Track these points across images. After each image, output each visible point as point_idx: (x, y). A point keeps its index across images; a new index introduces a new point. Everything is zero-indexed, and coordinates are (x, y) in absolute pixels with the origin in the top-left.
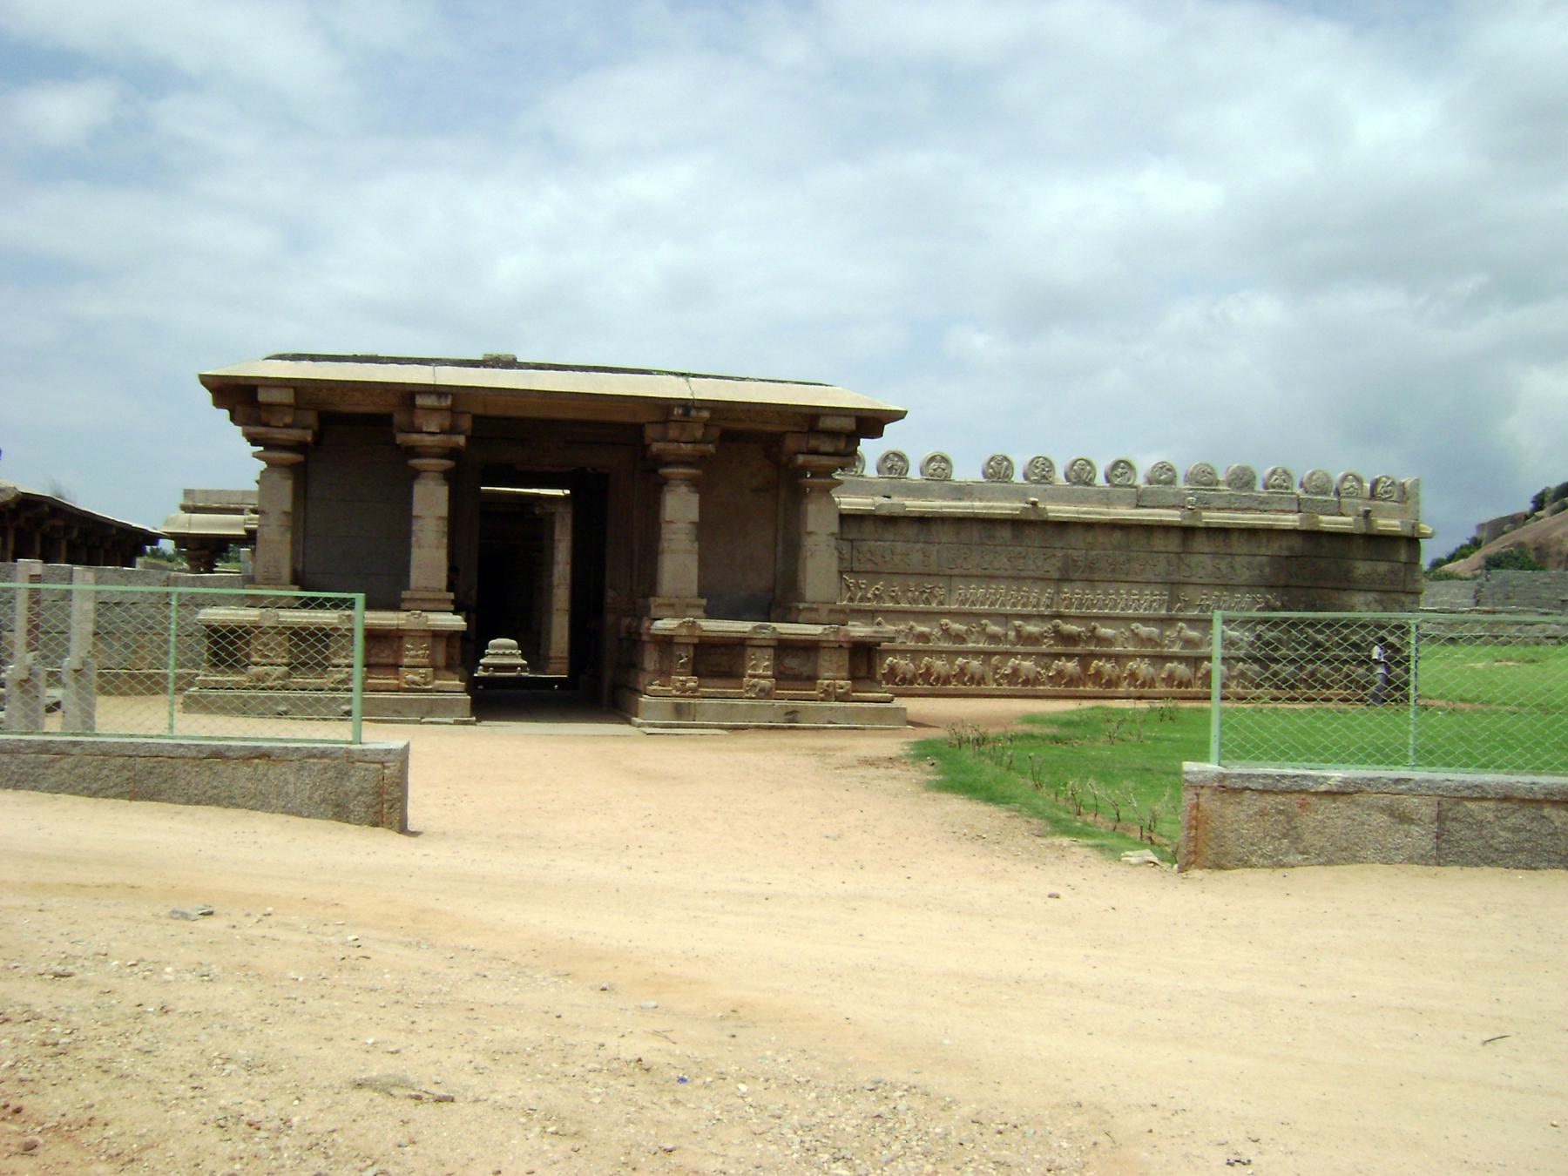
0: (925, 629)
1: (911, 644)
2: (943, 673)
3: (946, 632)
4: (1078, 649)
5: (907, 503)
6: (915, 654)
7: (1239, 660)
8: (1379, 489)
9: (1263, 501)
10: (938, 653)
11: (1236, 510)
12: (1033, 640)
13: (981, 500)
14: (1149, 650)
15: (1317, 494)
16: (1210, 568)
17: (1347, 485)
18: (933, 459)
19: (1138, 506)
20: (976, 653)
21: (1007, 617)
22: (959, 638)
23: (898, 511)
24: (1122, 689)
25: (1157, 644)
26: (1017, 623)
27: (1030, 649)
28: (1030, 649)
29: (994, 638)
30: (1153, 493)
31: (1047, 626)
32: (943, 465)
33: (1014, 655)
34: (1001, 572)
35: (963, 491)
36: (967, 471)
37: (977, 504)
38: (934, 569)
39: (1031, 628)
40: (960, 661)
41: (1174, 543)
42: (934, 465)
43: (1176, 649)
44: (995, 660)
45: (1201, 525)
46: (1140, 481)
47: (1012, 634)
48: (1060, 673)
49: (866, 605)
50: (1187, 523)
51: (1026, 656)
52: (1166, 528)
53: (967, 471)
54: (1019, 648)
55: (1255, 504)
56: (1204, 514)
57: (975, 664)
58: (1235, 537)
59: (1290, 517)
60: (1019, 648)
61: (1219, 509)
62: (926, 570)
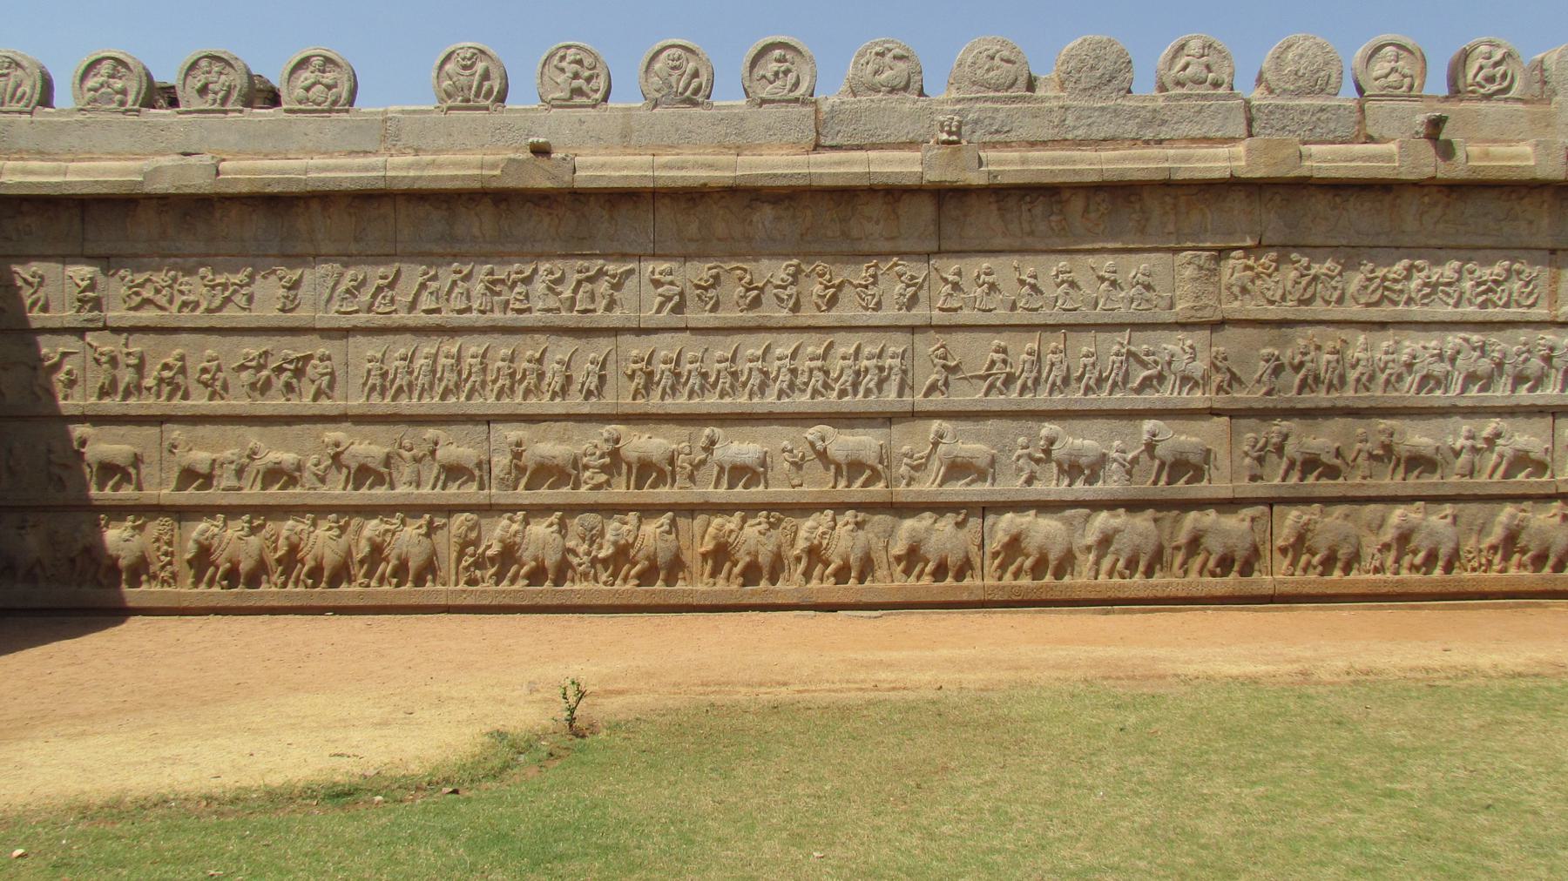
0: (288, 458)
1: (252, 493)
4: (665, 494)
7: (1096, 506)
9: (1156, 118)
11: (1080, 143)
14: (857, 491)
15: (1298, 93)
16: (1009, 290)
17: (1380, 67)
18: (303, 63)
19: (817, 147)
24: (790, 585)
26: (513, 433)
30: (856, 116)
34: (473, 318)
35: (387, 132)
38: (302, 315)
39: (549, 446)
40: (373, 527)
42: (306, 76)
43: (928, 486)
45: (976, 178)
46: (831, 96)
48: (622, 553)
49: (134, 405)
50: (933, 176)
54: (523, 495)
55: (1131, 129)
57: (408, 537)
58: (1077, 204)
59: (1223, 151)
62: (288, 320)
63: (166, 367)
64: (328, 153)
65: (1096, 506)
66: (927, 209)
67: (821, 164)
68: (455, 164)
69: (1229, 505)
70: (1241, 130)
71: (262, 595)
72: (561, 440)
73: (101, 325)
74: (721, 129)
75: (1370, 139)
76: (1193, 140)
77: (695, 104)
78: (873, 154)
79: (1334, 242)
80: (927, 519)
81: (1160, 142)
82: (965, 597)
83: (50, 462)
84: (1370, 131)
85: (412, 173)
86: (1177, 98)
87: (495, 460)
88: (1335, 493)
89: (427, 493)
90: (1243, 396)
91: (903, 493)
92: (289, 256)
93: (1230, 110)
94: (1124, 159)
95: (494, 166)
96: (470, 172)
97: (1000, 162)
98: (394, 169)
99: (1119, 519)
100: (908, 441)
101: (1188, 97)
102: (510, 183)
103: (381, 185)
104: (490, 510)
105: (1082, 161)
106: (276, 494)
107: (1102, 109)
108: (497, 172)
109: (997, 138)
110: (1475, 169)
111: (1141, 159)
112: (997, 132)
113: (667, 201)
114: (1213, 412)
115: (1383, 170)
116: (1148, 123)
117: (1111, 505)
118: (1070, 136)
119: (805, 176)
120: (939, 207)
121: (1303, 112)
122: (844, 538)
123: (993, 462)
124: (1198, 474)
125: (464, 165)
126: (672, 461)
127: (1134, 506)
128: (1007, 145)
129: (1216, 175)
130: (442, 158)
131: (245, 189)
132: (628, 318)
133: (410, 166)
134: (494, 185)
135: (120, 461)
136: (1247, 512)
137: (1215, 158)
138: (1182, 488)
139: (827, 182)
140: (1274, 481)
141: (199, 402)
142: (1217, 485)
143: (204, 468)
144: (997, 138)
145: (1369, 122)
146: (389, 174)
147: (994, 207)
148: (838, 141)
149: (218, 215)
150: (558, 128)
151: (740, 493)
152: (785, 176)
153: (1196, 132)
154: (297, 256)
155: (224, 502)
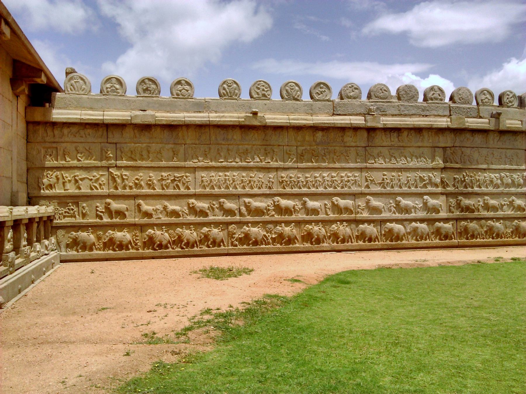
0: (177, 208)
2: (192, 240)
3: (193, 210)
4: (294, 217)
5: (157, 114)
6: (169, 226)
8: (505, 100)
10: (188, 225)
11: (406, 115)
12: (259, 212)
13: (216, 112)
19: (333, 114)
20: (217, 224)
21: (239, 196)
22: (203, 213)
23: (151, 121)
25: (351, 212)
26: (247, 200)
27: (257, 219)
28: (257, 219)
29: (229, 212)
31: (270, 202)
32: (187, 87)
33: (247, 223)
36: (206, 91)
37: (214, 115)
39: (256, 203)
40: (205, 229)
41: (362, 139)
43: (365, 215)
44: (231, 227)
45: (380, 126)
47: (243, 209)
49: (127, 191)
51: (255, 224)
52: (356, 129)
53: (206, 91)
56: (382, 118)
57: (215, 231)
58: (405, 133)
59: (445, 119)
60: (249, 218)
61: (393, 115)
63: (137, 179)
64: (188, 111)
65: (411, 220)
66: (365, 134)
67: (337, 120)
68: (230, 117)
69: (446, 220)
70: (448, 114)
71: (169, 252)
72: (261, 202)
73: (114, 165)
74: (306, 108)
75: (481, 117)
76: (435, 116)
77: (297, 100)
78: (351, 117)
79: (472, 146)
80: (366, 225)
81: (427, 116)
82: (376, 247)
83: (97, 210)
84: (481, 115)
85: (217, 119)
86: (431, 103)
87: (241, 208)
88: (473, 217)
89: (220, 218)
90: (450, 189)
91: (359, 216)
92: (176, 144)
93: (445, 107)
94: (419, 121)
95: (242, 118)
96: (235, 120)
97: (386, 121)
98: (212, 118)
99: (418, 225)
100: (361, 203)
101: (434, 103)
102: (247, 123)
103: (208, 123)
104: (240, 224)
105: (408, 121)
106: (173, 220)
107: (412, 106)
108: (243, 120)
109: (383, 113)
110: (508, 127)
111: (424, 121)
112: (383, 111)
113: (291, 129)
114: (442, 194)
115: (486, 126)
116: (423, 110)
117: (415, 220)
118: (402, 113)
119: (333, 123)
120: (368, 133)
121: (464, 109)
122: (344, 230)
123: (384, 208)
124: (438, 212)
125: (233, 117)
126: (294, 208)
127: (422, 221)
128: (386, 115)
129: (444, 126)
130: (226, 115)
131: (165, 123)
132: (280, 165)
133: (217, 117)
134: (243, 123)
135: (122, 210)
136: (451, 223)
137: (443, 122)
138: (434, 215)
139: (339, 125)
140: (457, 213)
141: (146, 191)
142: (443, 214)
143: (150, 212)
144: (383, 113)
145: (480, 112)
146: (211, 119)
147: (383, 133)
148: (339, 113)
149: (153, 131)
150: (257, 106)
151: (313, 217)
152: (327, 123)
153: (436, 114)
154: (179, 144)
155: (157, 222)
